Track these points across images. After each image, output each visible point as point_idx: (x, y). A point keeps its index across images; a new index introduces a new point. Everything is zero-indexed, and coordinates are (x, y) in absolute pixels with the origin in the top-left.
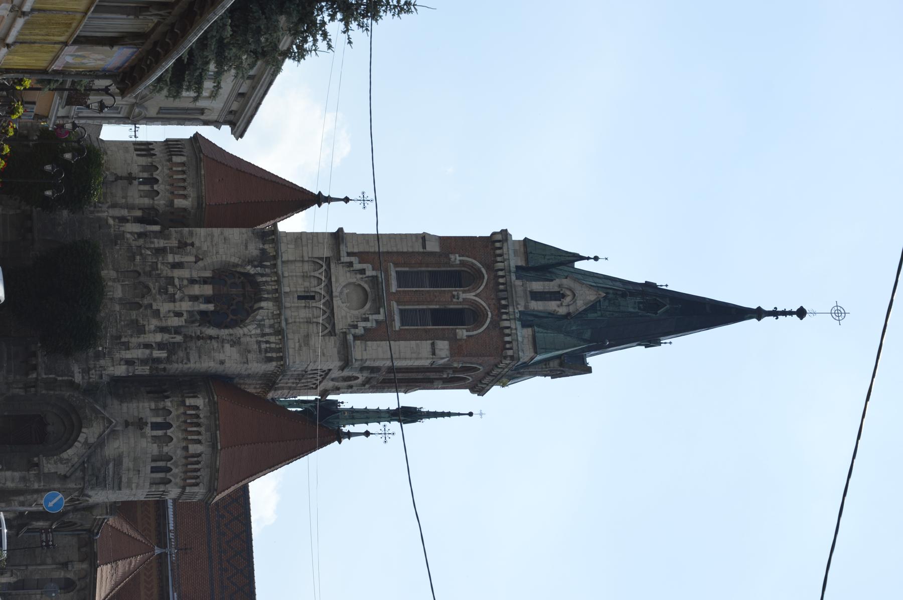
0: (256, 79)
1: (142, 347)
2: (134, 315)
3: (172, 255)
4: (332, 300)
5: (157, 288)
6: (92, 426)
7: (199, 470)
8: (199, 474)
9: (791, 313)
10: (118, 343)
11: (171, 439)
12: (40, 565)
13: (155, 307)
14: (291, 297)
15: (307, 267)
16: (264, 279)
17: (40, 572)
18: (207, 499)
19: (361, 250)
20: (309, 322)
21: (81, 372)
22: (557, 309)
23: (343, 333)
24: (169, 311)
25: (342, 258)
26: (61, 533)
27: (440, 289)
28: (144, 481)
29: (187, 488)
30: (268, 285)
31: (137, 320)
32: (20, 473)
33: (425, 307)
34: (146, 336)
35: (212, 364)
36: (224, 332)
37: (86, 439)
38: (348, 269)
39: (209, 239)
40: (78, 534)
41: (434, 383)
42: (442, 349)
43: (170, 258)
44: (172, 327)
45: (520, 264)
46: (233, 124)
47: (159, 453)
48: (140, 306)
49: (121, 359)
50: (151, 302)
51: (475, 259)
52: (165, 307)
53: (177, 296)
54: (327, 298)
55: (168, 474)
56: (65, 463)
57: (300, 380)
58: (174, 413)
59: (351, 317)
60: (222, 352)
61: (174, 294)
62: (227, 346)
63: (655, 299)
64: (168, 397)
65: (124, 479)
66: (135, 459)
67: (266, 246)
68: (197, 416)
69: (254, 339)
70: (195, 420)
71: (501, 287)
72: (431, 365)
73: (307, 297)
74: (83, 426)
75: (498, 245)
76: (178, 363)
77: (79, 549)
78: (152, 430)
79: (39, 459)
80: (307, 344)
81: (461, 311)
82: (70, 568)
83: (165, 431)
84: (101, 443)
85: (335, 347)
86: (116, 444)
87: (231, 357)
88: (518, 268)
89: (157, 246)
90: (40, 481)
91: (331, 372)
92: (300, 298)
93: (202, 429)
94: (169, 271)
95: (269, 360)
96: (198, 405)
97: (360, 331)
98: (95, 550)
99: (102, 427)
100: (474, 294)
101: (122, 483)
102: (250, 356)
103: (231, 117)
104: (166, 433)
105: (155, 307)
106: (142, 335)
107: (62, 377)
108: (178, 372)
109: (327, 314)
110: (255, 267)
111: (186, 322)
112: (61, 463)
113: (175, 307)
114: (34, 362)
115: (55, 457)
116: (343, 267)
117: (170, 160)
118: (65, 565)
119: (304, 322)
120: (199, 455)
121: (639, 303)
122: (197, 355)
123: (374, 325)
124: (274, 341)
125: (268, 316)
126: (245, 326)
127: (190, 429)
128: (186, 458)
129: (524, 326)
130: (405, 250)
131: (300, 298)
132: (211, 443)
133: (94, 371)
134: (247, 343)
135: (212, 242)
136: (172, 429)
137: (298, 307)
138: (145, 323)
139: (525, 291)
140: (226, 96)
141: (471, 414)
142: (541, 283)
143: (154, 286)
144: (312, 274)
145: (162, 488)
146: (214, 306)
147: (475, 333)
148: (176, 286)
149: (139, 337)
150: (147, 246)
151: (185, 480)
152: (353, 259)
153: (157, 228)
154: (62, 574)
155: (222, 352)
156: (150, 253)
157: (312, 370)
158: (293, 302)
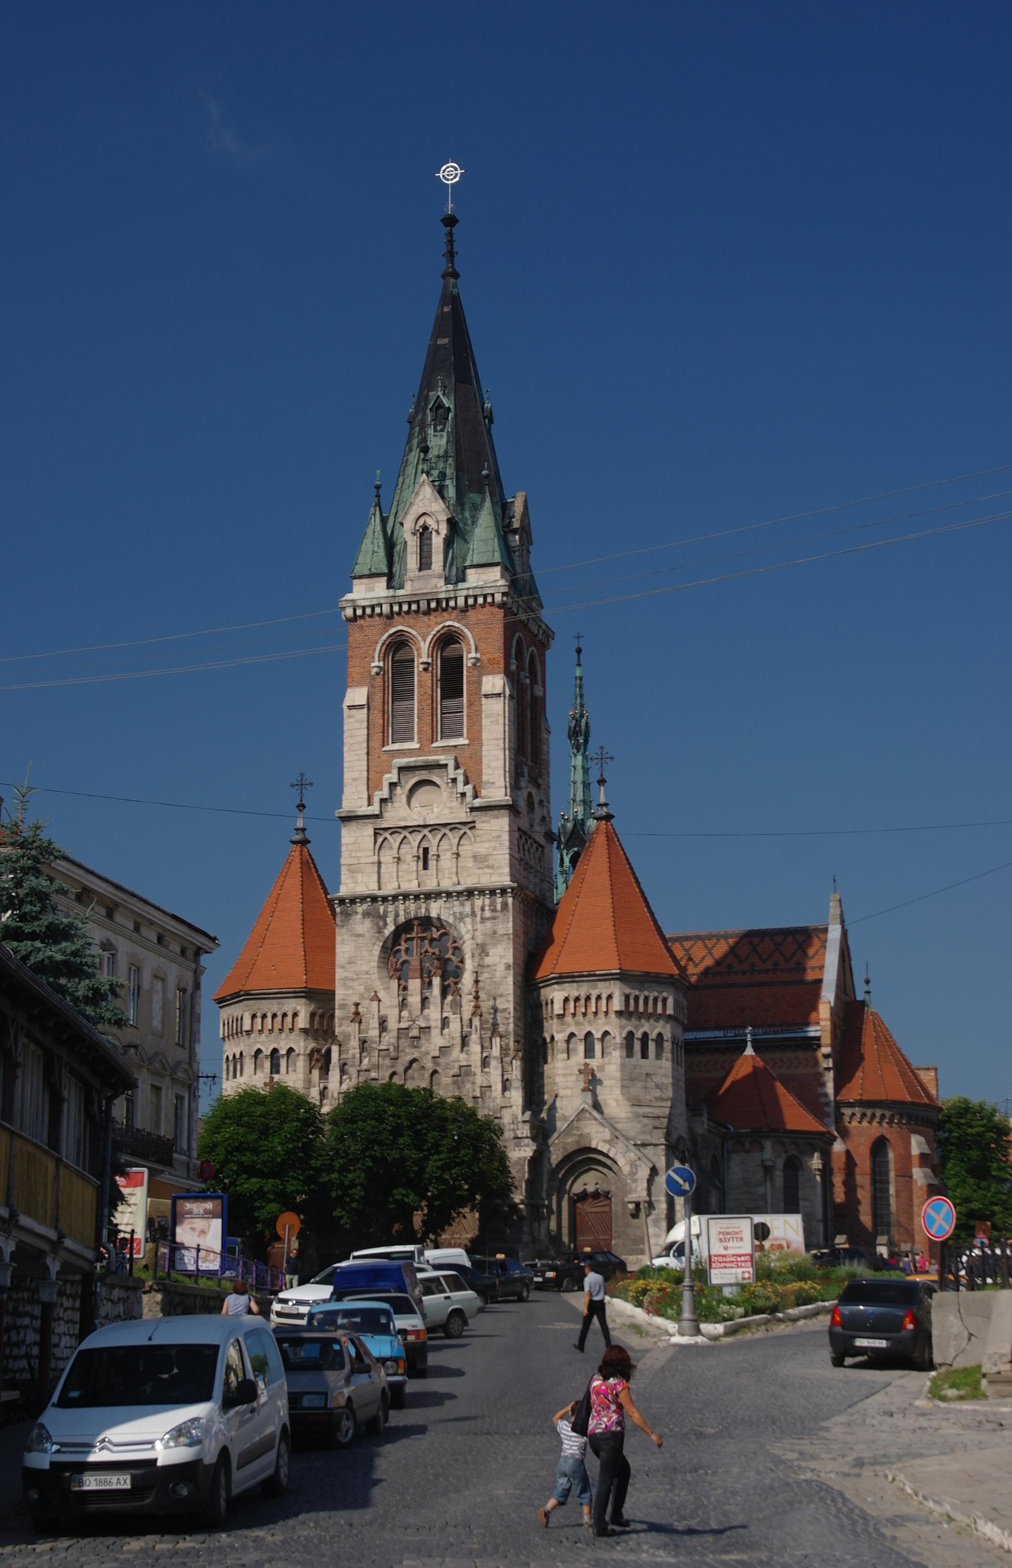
0: (140, 920)
1: (487, 1070)
3: (370, 1031)
5: (413, 1050)
7: (646, 999)
12: (766, 1202)
14: (425, 878)
15: (387, 857)
16: (402, 913)
19: (365, 787)
23: (471, 811)
24: (442, 1033)
27: (416, 688)
31: (453, 1076)
35: (510, 980)
36: (469, 965)
37: (605, 1141)
39: (350, 983)
40: (728, 1152)
42: (493, 684)
43: (374, 1033)
45: (385, 584)
46: (199, 951)
50: (430, 1057)
51: (377, 643)
52: (436, 1040)
53: (423, 1025)
56: (636, 1169)
57: (532, 868)
59: (451, 802)
60: (494, 968)
61: (421, 1028)
62: (488, 960)
63: (431, 409)
64: (552, 1038)
68: (577, 999)
69: (479, 926)
70: (582, 1002)
71: (414, 607)
75: (359, 612)
76: (508, 1024)
77: (747, 1152)
82: (770, 1163)
83: (596, 1041)
84: (610, 1123)
86: (613, 1103)
88: (389, 586)
89: (358, 1051)
90: (658, 1201)
92: (425, 867)
94: (391, 1035)
96: (563, 998)
97: (469, 789)
98: (748, 1130)
99: (590, 1122)
100: (422, 643)
102: (501, 932)
103: (190, 953)
106: (473, 1069)
108: (522, 1026)
109: (447, 831)
110: (386, 924)
112: (636, 1173)
113: (436, 1027)
117: (249, 1033)
120: (627, 997)
121: (435, 430)
123: (461, 771)
124: (481, 900)
125: (449, 908)
127: (594, 1010)
129: (463, 579)
131: (425, 867)
135: (353, 980)
136: (593, 1032)
138: (457, 1066)
139: (419, 578)
140: (162, 959)
141: (579, 651)
142: (409, 556)
147: (472, 642)
149: (475, 1074)
150: (358, 1063)
152: (376, 800)
153: (335, 1049)
154: (779, 1174)
155: (494, 968)
156: (367, 1060)
157: (519, 852)
158: (432, 876)
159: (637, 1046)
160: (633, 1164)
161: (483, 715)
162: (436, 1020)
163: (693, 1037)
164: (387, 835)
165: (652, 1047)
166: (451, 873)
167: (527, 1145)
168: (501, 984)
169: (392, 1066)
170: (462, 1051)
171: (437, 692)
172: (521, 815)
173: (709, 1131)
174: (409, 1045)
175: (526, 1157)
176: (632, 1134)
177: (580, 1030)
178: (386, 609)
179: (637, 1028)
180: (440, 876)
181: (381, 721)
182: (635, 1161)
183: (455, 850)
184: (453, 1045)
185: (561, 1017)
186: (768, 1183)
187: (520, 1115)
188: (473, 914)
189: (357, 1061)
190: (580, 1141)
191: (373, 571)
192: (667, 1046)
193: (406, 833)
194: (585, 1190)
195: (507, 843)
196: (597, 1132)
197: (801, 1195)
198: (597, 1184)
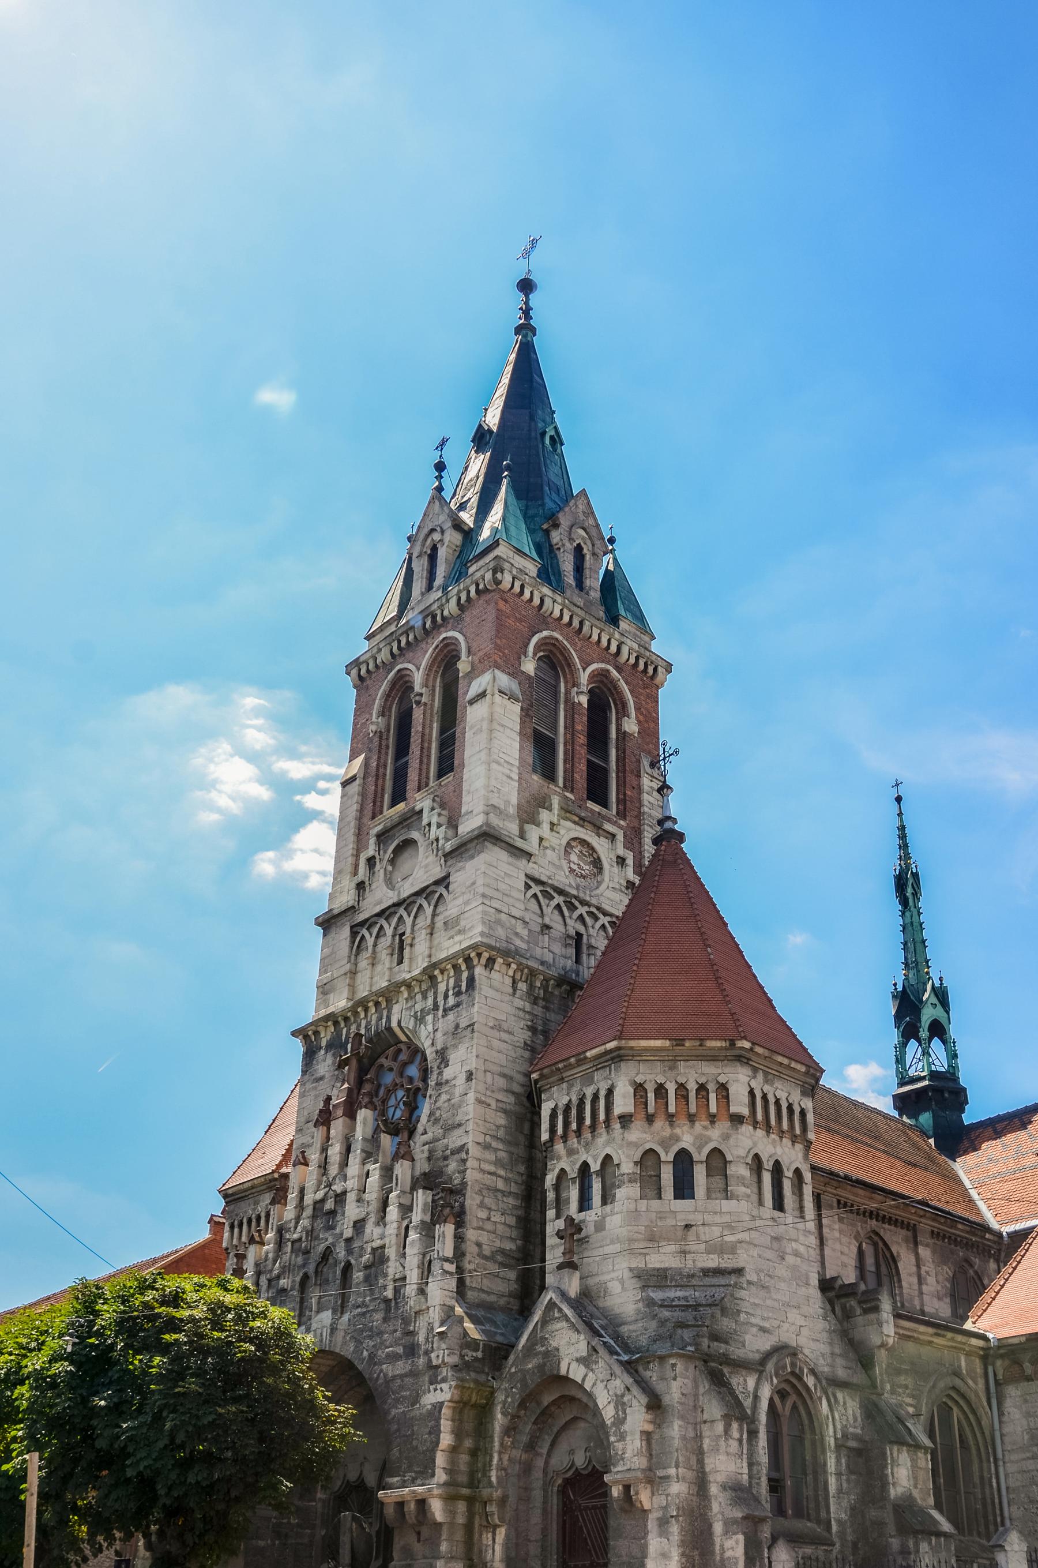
4: (404, 900)
7: (681, 1087)
8: (692, 1087)
10: (397, 1303)
11: (608, 1158)
18: (796, 1076)
21: (434, 1386)
26: (997, 1426)
28: (716, 1213)
29: (733, 1109)
32: (650, 1536)
35: (471, 1097)
37: (580, 1360)
38: (367, 889)
40: (997, 1383)
41: (627, 730)
44: (383, 1190)
55: (696, 1157)
56: (625, 1412)
58: (564, 1164)
59: (427, 857)
60: (453, 1082)
62: (448, 1073)
66: (653, 1239)
68: (568, 1108)
70: (574, 1112)
72: (517, 700)
74: (555, 1372)
77: (1029, 1379)
79: (616, 1482)
80: (457, 920)
83: (594, 1176)
85: (463, 868)
86: (615, 1287)
90: (666, 1478)
91: (544, 879)
92: (400, 962)
93: (589, 1092)
99: (559, 1325)
101: (723, 1265)
106: (386, 1250)
115: (612, 1439)
119: (431, 940)
120: (639, 1089)
124: (445, 983)
127: (588, 1122)
136: (590, 1161)
145: (739, 1170)
146: (361, 1109)
151: (712, 1119)
160: (620, 1403)
162: (353, 1177)
165: (700, 1173)
166: (423, 959)
167: (444, 1380)
171: (431, 728)
182: (623, 1396)
187: (437, 1324)
188: (436, 1007)
190: (545, 1364)
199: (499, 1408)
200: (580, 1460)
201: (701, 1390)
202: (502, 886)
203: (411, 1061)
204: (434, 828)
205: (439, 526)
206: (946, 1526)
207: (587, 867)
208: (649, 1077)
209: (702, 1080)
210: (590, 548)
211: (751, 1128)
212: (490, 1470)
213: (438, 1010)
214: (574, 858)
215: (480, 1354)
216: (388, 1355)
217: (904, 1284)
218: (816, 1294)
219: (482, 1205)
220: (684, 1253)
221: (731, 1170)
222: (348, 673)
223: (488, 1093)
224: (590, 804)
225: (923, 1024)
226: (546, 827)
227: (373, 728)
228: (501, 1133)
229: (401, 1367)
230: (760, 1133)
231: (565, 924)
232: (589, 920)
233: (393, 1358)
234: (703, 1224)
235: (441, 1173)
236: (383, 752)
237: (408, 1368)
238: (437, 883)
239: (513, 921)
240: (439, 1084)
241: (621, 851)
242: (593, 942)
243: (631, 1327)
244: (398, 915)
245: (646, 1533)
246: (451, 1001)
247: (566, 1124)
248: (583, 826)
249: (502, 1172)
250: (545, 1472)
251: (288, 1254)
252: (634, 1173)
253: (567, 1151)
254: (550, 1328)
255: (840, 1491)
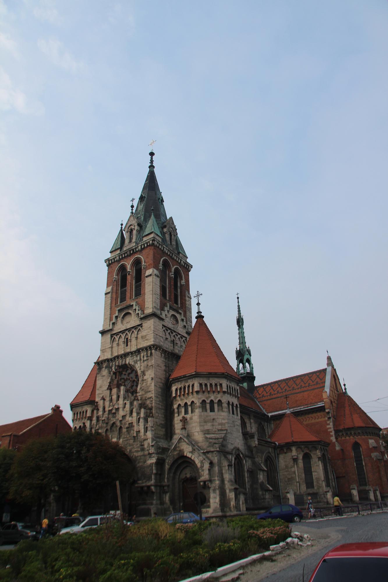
2: (124, 430)
4: (128, 329)
5: (114, 419)
6: (183, 449)
7: (211, 385)
8: (214, 384)
9: (152, 158)
10: (137, 438)
12: (296, 475)
13: (121, 419)
15: (115, 344)
17: (300, 474)
20: (137, 338)
21: (151, 458)
22: (136, 230)
23: (141, 320)
25: (111, 328)
28: (220, 416)
29: (224, 390)
30: (120, 361)
31: (127, 428)
33: (134, 286)
34: (133, 421)
35: (153, 384)
37: (190, 452)
38: (116, 325)
40: (278, 454)
43: (100, 413)
47: (200, 408)
48: (121, 428)
49: (145, 435)
52: (121, 413)
53: (117, 407)
54: (127, 332)
56: (203, 464)
58: (180, 402)
59: (135, 318)
60: (147, 380)
62: (145, 377)
65: (220, 427)
67: (104, 366)
68: (180, 389)
69: (142, 364)
70: (183, 389)
72: (159, 277)
73: (127, 342)
74: (183, 455)
76: (152, 403)
77: (286, 453)
78: (188, 414)
79: (202, 481)
81: (136, 270)
82: (295, 457)
83: (189, 406)
84: (193, 444)
85: (147, 322)
86: (196, 434)
87: (150, 375)
88: (120, 251)
89: (95, 421)
90: (215, 480)
91: (166, 326)
92: (127, 345)
93: (187, 385)
95: (151, 354)
96: (175, 389)
97: (140, 312)
104: (190, 405)
105: (121, 419)
107: (153, 470)
111: (128, 401)
112: (203, 467)
114: (146, 488)
115: (200, 471)
116: (114, 327)
118: (295, 460)
119: (137, 341)
120: (201, 385)
121: (140, 204)
122: (149, 393)
124: (143, 353)
125: (132, 359)
126: (137, 370)
127: (187, 392)
128: (204, 392)
130: (110, 301)
132: (194, 379)
133: (150, 451)
134: (144, 367)
136: (188, 402)
137: (130, 346)
138: (128, 423)
141: (238, 298)
143: (113, 420)
144: (117, 341)
145: (225, 405)
146: (122, 386)
148: (113, 408)
151: (219, 392)
159: (208, 406)
160: (202, 462)
161: (146, 284)
162: (121, 404)
163: (278, 413)
164: (115, 336)
165: (216, 406)
166: (135, 346)
167: (153, 457)
168: (150, 386)
169: (106, 427)
170: (130, 417)
171: (133, 281)
172: (165, 321)
173: (258, 444)
174: (112, 417)
175: (154, 463)
176: (205, 447)
177: (183, 402)
178: (118, 258)
179: (207, 398)
180: (132, 347)
181: (115, 296)
182: (203, 460)
183: (136, 336)
184: (127, 414)
185: (175, 397)
186: (296, 466)
188: (140, 359)
189: (95, 426)
191: (116, 248)
192: (225, 405)
193: (121, 334)
194: (186, 477)
195: (153, 329)
196: (186, 448)
197: (313, 470)
198: (190, 473)
199: (167, 463)
200: (188, 476)
201: (222, 459)
202: (157, 328)
203: (131, 373)
204: (137, 311)
205: (133, 224)
206: (271, 488)
207: (174, 322)
208: (203, 382)
209: (216, 383)
210: (173, 233)
211: (227, 394)
212: (165, 479)
213: (141, 360)
214: (172, 319)
215: (161, 450)
216: (135, 451)
217: (248, 429)
218: (241, 435)
219: (157, 412)
220: (213, 425)
221: (223, 405)
222: (106, 262)
223: (157, 383)
224: (175, 305)
225: (244, 359)
226: (166, 312)
227: (114, 279)
228: (160, 394)
229: (140, 453)
230: (229, 395)
231: (171, 337)
232: (176, 336)
233: (137, 451)
234: (217, 418)
235: (145, 404)
236: (118, 286)
237: (142, 454)
238: (139, 325)
239: (160, 337)
240: (143, 380)
241: (183, 318)
242: (177, 342)
243: (202, 444)
244: (126, 333)
245: (210, 493)
246: (145, 358)
247: (180, 392)
248: (174, 311)
249: (161, 404)
250: (179, 479)
251: (101, 423)
252: (200, 406)
253: (181, 399)
254: (181, 444)
255: (248, 481)
